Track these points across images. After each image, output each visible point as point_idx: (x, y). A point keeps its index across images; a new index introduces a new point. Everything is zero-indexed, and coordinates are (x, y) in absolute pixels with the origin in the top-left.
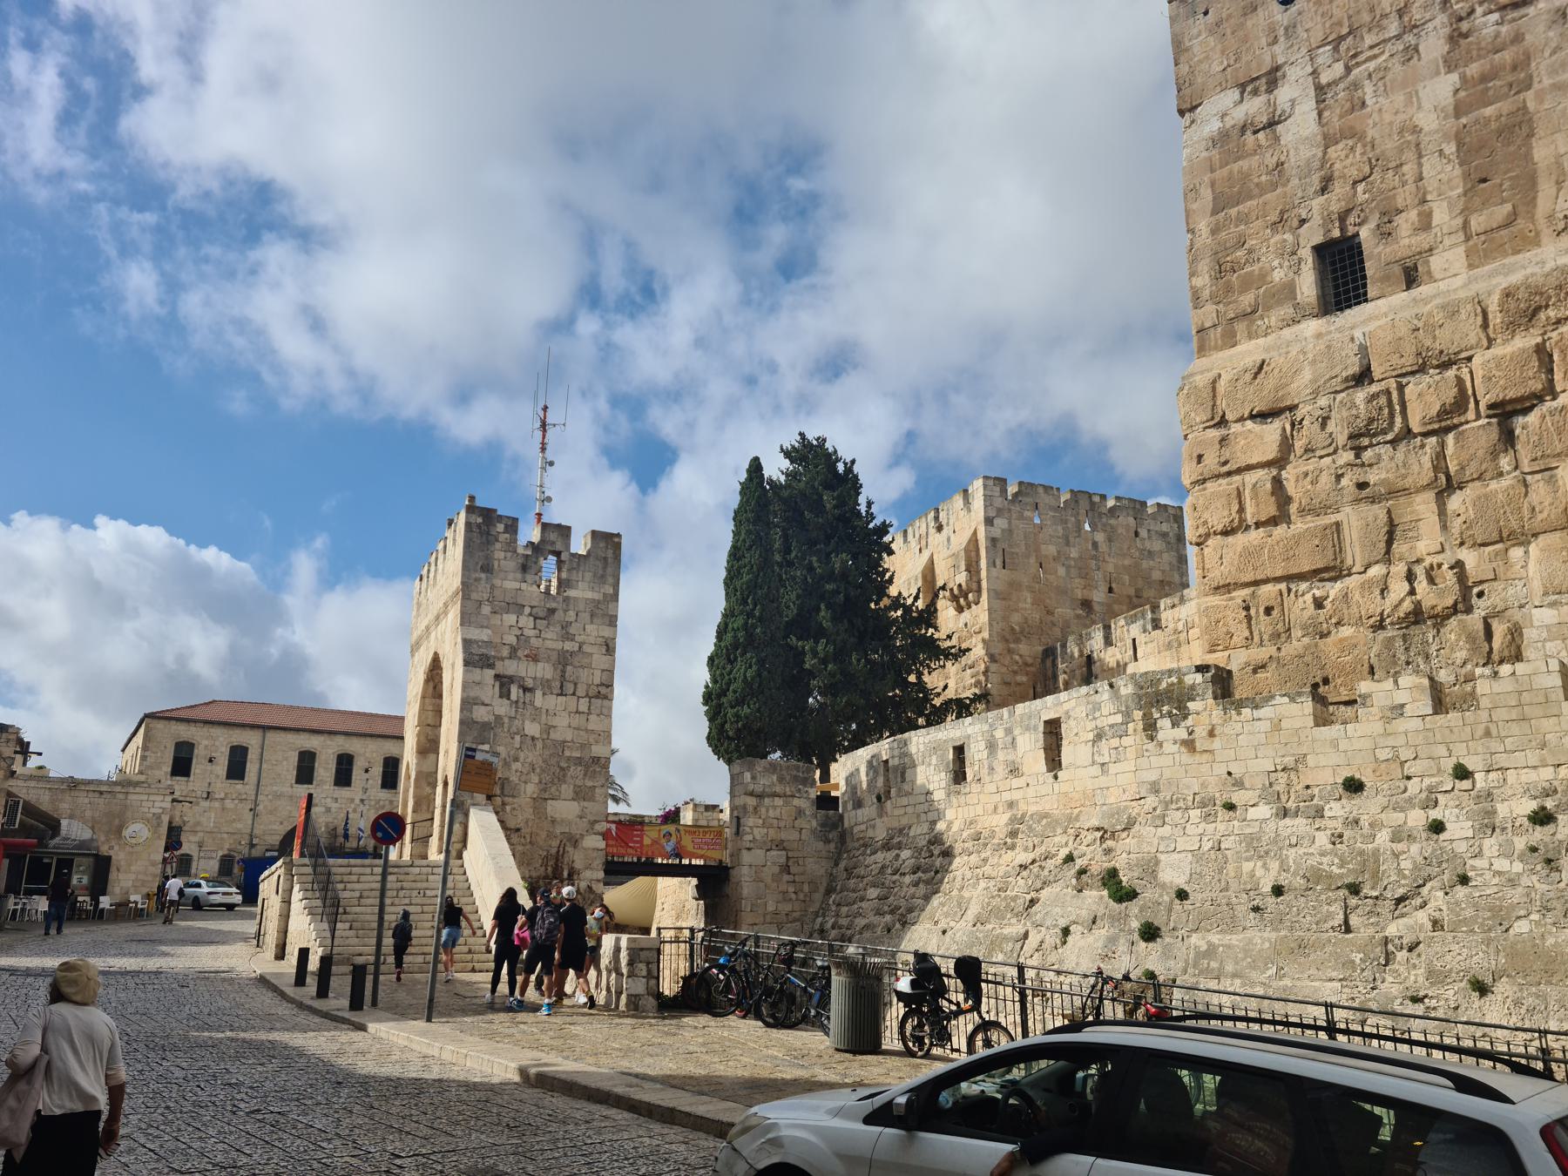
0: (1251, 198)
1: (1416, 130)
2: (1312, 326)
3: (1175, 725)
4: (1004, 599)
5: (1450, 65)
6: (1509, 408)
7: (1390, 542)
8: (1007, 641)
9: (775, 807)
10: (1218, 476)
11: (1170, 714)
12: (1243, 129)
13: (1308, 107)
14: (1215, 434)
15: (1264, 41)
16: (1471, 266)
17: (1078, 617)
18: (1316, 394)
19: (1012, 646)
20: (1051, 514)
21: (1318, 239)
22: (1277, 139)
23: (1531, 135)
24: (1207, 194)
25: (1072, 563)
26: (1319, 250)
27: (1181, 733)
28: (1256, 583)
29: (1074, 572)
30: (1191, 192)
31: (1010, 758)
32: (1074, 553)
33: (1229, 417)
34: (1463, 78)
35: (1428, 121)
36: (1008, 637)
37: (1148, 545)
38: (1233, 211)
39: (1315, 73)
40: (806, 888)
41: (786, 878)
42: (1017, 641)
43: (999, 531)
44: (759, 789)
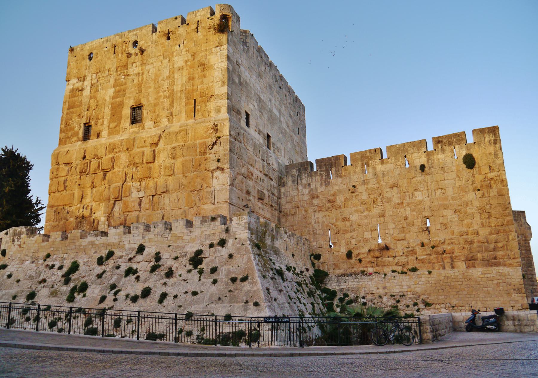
0: (75, 108)
1: (106, 101)
2: (80, 143)
3: (18, 241)
5: (114, 86)
6: (106, 171)
7: (82, 199)
10: (56, 178)
11: (18, 238)
12: (77, 90)
13: (89, 87)
14: (56, 166)
15: (84, 68)
16: (108, 136)
18: (76, 160)
21: (85, 122)
22: (82, 94)
23: (123, 107)
24: (67, 103)
26: (85, 124)
27: (19, 243)
28: (58, 206)
30: (64, 103)
33: (60, 163)
34: (115, 89)
35: (108, 99)
38: (71, 110)
39: (92, 80)
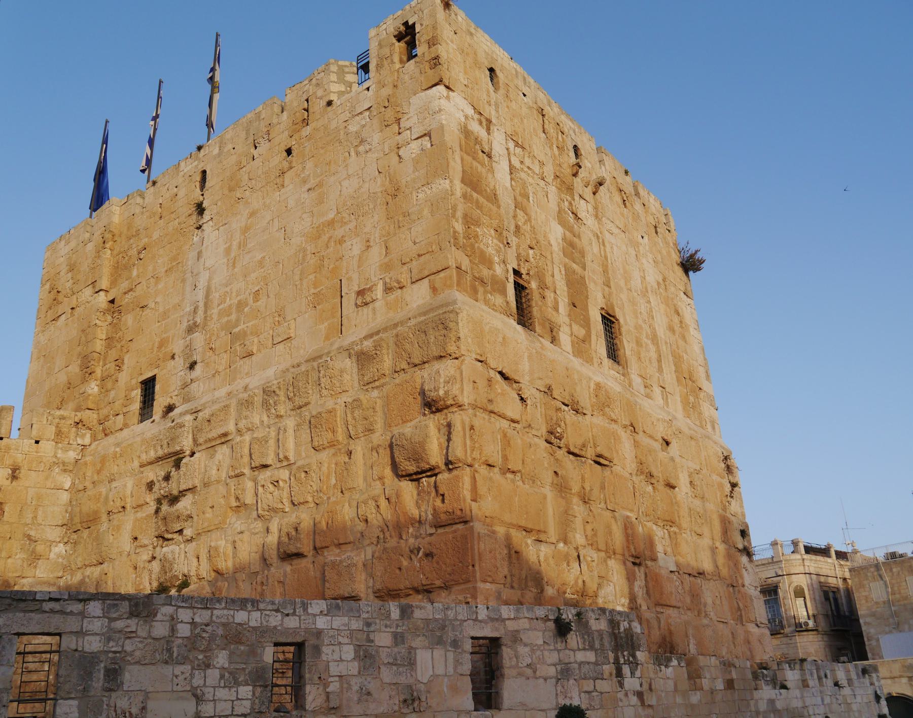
31: (403, 680)
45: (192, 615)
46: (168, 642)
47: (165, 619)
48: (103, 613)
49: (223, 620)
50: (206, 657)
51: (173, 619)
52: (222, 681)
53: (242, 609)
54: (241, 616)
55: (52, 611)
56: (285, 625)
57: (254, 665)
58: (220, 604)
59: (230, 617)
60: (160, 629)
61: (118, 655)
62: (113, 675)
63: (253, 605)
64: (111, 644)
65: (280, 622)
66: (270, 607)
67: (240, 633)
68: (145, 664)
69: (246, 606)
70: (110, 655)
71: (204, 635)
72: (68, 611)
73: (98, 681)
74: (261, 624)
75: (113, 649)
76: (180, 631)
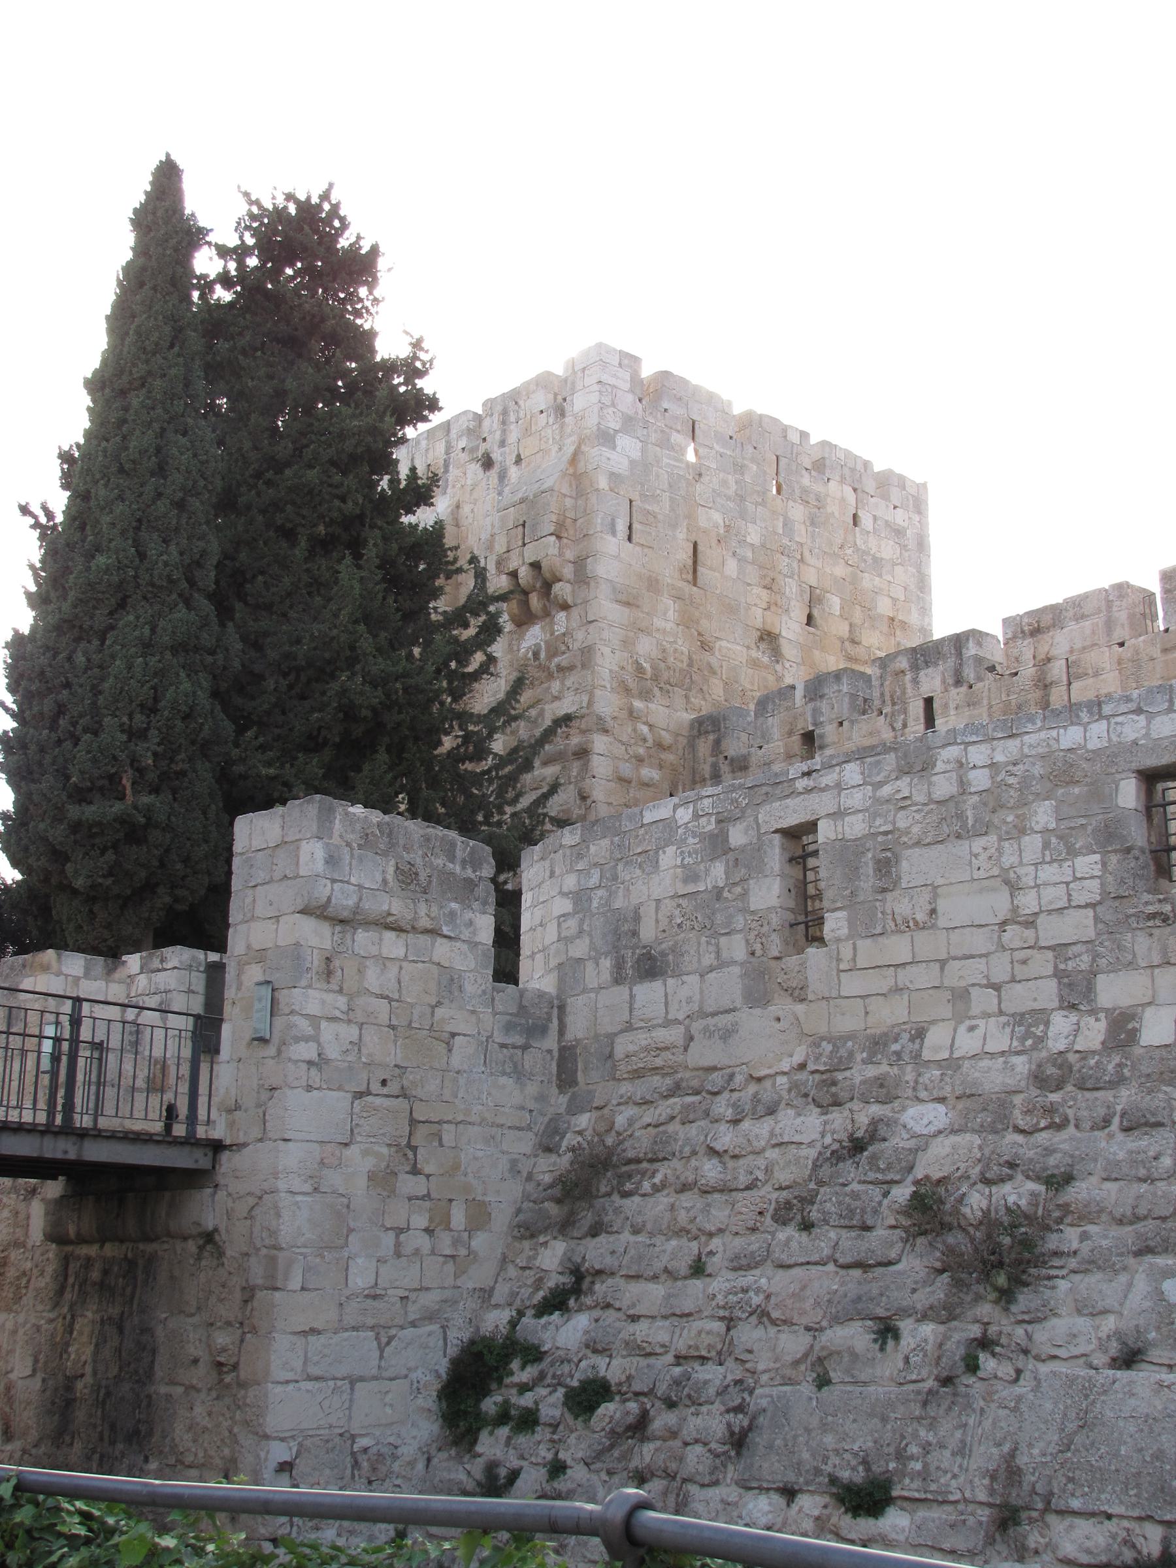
4: (628, 604)
8: (627, 690)
9: (384, 961)
17: (755, 664)
19: (638, 704)
20: (717, 447)
25: (749, 555)
29: (752, 574)
32: (754, 536)
36: (632, 683)
37: (873, 543)
40: (458, 1217)
41: (409, 1185)
42: (646, 695)
43: (626, 462)
44: (344, 900)
45: (989, 752)
46: (957, 803)
47: (949, 767)
48: (864, 779)
49: (1040, 750)
50: (1017, 816)
51: (961, 765)
52: (1047, 852)
53: (1072, 724)
54: (1071, 736)
55: (808, 791)
56: (1154, 735)
57: (1101, 817)
58: (1034, 723)
59: (1052, 742)
60: (944, 786)
61: (890, 836)
62: (886, 866)
63: (1090, 712)
64: (878, 822)
65: (1144, 731)
66: (1124, 708)
67: (1072, 766)
68: (929, 844)
69: (1078, 716)
70: (880, 839)
71: (1011, 780)
72: (823, 785)
73: (868, 881)
74: (1110, 740)
75: (882, 829)
76: (974, 783)
